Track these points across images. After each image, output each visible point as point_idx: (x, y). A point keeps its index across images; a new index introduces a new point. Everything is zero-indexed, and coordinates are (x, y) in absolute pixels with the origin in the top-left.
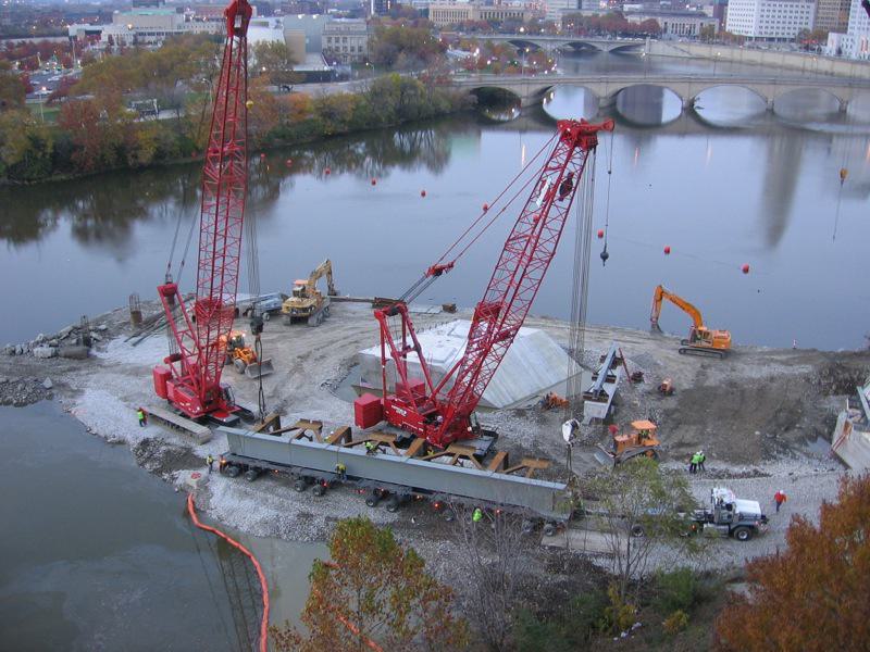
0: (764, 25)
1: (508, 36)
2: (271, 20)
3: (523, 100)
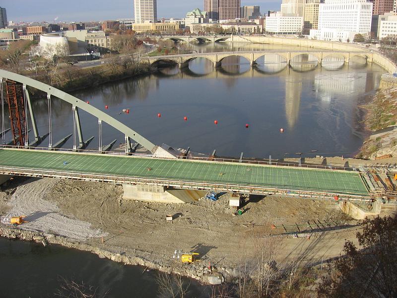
0: (282, 27)
1: (169, 36)
2: (60, 34)
3: (180, 65)
